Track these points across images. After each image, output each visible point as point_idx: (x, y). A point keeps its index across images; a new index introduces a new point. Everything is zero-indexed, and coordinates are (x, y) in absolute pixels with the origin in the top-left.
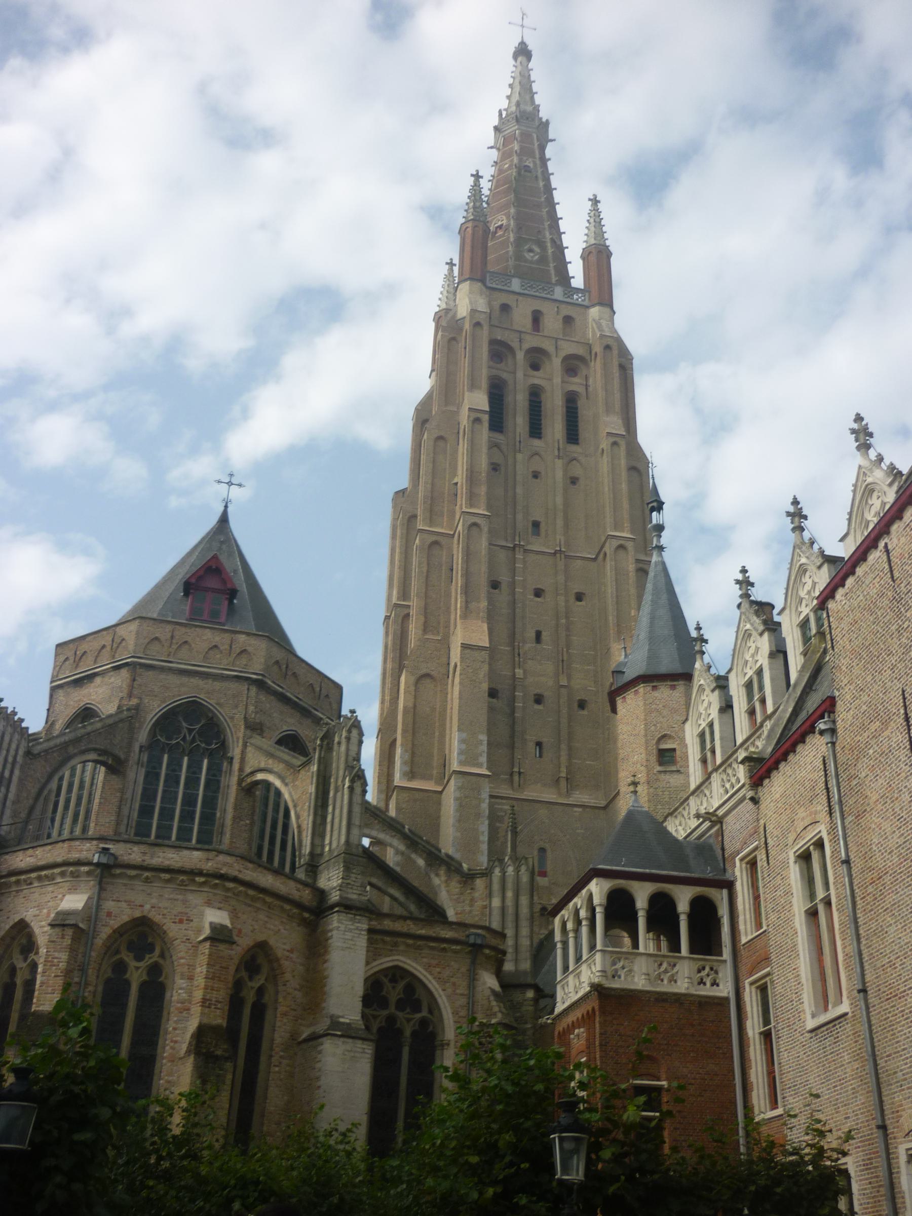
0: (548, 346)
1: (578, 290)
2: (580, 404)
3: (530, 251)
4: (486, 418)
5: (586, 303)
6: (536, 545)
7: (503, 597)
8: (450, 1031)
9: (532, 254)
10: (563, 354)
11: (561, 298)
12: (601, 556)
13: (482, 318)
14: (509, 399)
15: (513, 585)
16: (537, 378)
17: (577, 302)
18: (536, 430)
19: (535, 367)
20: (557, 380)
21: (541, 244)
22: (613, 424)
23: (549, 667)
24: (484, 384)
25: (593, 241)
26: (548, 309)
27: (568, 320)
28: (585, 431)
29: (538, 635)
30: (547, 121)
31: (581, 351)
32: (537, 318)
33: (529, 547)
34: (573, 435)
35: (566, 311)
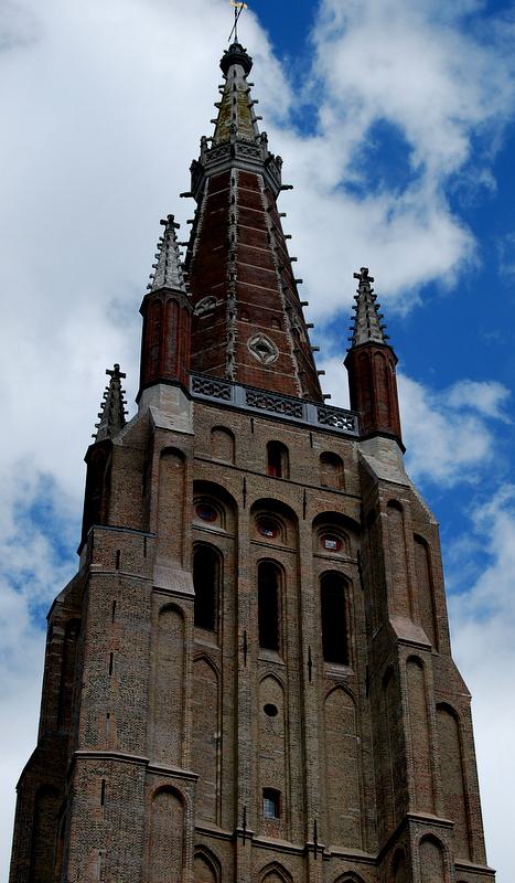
0: (292, 500)
1: (340, 412)
3: (261, 347)
4: (188, 608)
5: (356, 433)
9: (262, 353)
10: (313, 512)
11: (317, 424)
12: (389, 859)
13: (179, 443)
16: (273, 547)
17: (340, 430)
18: (270, 636)
24: (189, 553)
25: (363, 339)
26: (293, 440)
30: (279, 158)
33: (260, 839)
35: (323, 444)
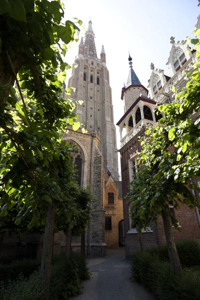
2: (100, 78)
6: (91, 100)
7: (85, 108)
8: (87, 158)
14: (87, 75)
15: (87, 106)
18: (91, 81)
19: (92, 71)
20: (96, 73)
21: (93, 52)
22: (106, 81)
23: (93, 121)
26: (95, 62)
27: (98, 64)
28: (100, 83)
29: (91, 116)
31: (100, 69)
32: (92, 64)
34: (98, 83)
